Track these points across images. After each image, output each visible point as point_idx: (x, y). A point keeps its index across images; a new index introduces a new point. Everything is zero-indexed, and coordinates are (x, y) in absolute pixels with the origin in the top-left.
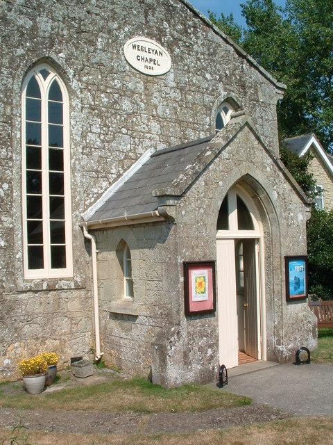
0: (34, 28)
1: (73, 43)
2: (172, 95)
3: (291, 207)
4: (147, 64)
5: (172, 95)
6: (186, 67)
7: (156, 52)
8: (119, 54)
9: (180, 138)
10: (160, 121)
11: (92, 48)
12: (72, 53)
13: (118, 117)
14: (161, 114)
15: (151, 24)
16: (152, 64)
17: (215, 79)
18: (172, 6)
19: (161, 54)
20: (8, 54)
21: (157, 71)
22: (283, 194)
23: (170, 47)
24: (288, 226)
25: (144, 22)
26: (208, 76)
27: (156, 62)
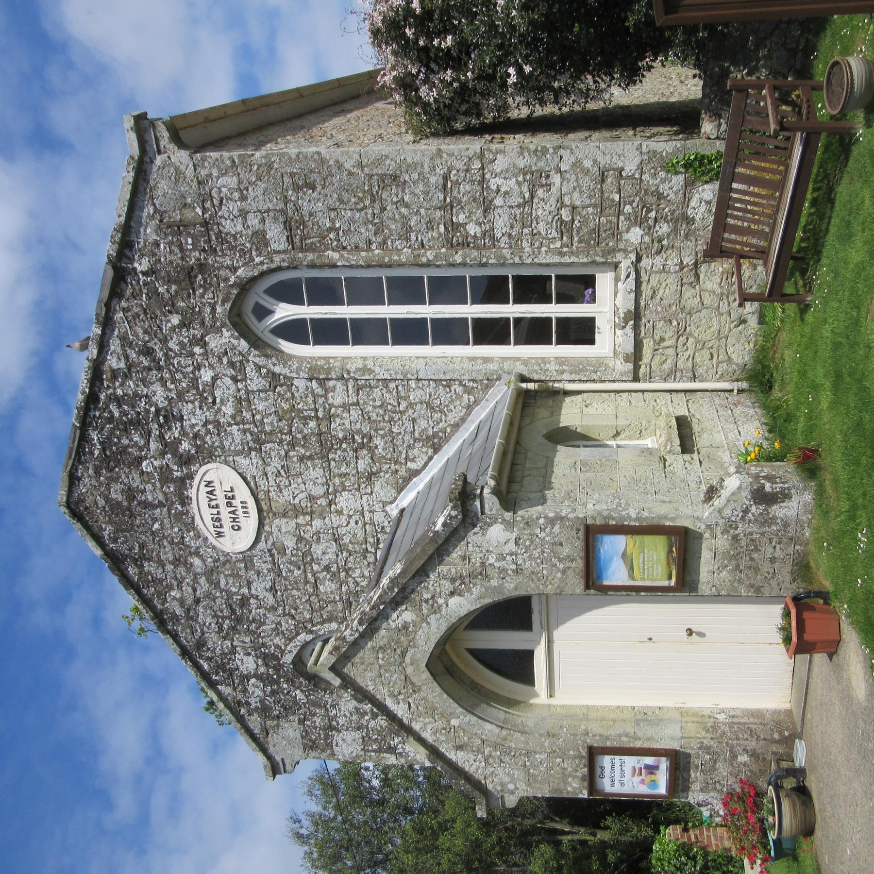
0: (257, 676)
1: (258, 628)
2: (276, 464)
3: (476, 559)
4: (240, 512)
5: (276, 464)
6: (210, 427)
7: (211, 493)
8: (247, 558)
9: (356, 451)
10: (336, 491)
11: (252, 601)
12: (273, 630)
13: (350, 565)
14: (319, 491)
15: (161, 497)
16: (236, 503)
17: (205, 355)
18: (104, 450)
19: (209, 484)
20: (309, 709)
21: (243, 493)
22: (453, 580)
23: (186, 460)
25: (165, 509)
26: (206, 375)
27: (230, 494)
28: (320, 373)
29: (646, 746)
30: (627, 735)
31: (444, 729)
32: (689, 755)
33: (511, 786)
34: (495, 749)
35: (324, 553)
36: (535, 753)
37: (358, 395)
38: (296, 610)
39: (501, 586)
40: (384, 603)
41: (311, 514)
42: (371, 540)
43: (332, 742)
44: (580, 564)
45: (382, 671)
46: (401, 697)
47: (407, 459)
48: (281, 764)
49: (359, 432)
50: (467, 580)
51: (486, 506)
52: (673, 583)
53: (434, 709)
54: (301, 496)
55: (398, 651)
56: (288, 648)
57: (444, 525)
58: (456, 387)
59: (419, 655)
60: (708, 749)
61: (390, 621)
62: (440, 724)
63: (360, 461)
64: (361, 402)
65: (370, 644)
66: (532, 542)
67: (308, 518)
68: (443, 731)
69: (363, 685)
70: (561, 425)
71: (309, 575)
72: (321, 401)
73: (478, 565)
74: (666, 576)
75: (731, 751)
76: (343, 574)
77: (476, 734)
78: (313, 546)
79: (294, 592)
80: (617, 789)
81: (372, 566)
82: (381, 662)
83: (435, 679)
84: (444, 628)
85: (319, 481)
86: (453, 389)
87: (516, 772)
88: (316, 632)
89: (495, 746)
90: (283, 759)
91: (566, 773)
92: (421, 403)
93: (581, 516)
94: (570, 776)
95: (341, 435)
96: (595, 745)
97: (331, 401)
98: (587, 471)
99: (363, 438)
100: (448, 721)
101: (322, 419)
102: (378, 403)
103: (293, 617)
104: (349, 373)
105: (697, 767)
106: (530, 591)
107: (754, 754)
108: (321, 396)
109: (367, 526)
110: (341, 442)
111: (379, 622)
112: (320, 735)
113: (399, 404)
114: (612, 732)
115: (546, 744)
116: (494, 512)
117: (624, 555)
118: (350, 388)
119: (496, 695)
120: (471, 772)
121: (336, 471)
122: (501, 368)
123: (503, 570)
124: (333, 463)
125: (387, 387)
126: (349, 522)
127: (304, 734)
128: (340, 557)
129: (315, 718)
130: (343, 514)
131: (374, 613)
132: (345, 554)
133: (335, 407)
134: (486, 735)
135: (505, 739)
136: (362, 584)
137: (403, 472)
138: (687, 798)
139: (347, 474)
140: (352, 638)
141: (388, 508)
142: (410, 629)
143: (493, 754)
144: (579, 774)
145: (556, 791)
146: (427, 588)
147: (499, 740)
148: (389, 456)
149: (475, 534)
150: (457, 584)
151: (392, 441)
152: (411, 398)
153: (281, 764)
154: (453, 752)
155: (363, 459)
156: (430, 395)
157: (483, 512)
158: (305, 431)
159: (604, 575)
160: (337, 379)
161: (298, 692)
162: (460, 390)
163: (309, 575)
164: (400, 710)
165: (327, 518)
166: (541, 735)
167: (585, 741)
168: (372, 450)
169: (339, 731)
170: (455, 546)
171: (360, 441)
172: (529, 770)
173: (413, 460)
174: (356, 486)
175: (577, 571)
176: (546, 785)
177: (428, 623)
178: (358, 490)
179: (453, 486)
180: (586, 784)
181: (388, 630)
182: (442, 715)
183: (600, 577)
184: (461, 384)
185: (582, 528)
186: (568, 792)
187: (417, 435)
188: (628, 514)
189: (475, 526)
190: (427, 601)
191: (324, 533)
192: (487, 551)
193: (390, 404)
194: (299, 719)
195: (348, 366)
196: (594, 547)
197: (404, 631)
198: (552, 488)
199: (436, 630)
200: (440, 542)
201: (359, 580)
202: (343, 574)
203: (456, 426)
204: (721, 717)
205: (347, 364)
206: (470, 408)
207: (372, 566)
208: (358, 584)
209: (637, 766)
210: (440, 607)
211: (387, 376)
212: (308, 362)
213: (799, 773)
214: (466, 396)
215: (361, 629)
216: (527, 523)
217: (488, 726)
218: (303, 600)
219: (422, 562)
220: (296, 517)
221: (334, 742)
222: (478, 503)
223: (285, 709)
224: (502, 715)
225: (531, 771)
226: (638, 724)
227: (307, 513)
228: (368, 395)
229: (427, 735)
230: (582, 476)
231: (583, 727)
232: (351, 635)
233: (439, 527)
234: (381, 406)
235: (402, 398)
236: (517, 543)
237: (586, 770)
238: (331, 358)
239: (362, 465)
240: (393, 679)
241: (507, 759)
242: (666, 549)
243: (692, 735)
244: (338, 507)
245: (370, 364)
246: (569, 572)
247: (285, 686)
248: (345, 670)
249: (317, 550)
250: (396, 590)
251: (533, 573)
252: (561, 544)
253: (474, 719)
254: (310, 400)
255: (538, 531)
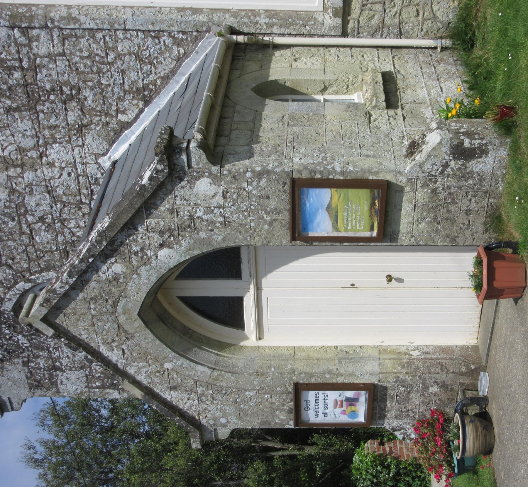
3: (184, 212)
9: (65, 102)
10: (46, 144)
13: (65, 216)
14: (29, 143)
20: (32, 352)
22: (162, 233)
24: (226, 223)
28: (21, 21)
29: (346, 381)
30: (330, 372)
31: (158, 372)
32: (386, 388)
33: (223, 421)
34: (207, 388)
35: (37, 205)
36: (245, 390)
37: (64, 45)
38: (13, 259)
39: (209, 238)
40: (93, 256)
41: (22, 166)
42: (85, 191)
43: (56, 382)
44: (286, 216)
45: (95, 321)
46: (115, 344)
47: (117, 111)
48: (8, 403)
49: (67, 83)
50: (176, 233)
51: (193, 160)
52: (374, 234)
53: (147, 354)
54: (11, 148)
55: (110, 302)
56: (8, 296)
57: (151, 178)
58: (165, 39)
59: (130, 304)
60: (402, 383)
61: (100, 273)
62: (154, 367)
63: (70, 113)
64: (68, 52)
65: (81, 296)
66: (239, 195)
67: (19, 170)
68: (157, 374)
69: (76, 334)
70: (271, 79)
71: (24, 227)
72: (25, 50)
73: (186, 217)
74: (368, 228)
75: (423, 384)
76: (58, 225)
77: (189, 376)
78: (27, 198)
79: (10, 243)
80: (321, 419)
81: (87, 217)
82: (93, 312)
83: (147, 326)
84: (154, 279)
85: (29, 133)
86: (162, 40)
87: (228, 408)
88: (34, 281)
89: (208, 385)
90: (9, 399)
91: (274, 407)
92: (130, 55)
93: (288, 169)
94: (278, 409)
95: (48, 87)
96: (301, 382)
97: (35, 50)
98: (294, 125)
99: (71, 90)
100: (162, 365)
101: (27, 70)
102: (86, 54)
103: (10, 267)
104: (53, 21)
105: (392, 398)
106: (238, 243)
107: (443, 386)
108: (25, 46)
109: (80, 178)
110: (49, 93)
111: (89, 274)
112: (44, 375)
113: (107, 54)
114: (316, 370)
115: (255, 382)
116: (201, 165)
117: (329, 208)
118: (55, 37)
119: (208, 339)
120: (185, 409)
121: (46, 123)
122: (211, 20)
123: (211, 223)
124: (41, 115)
125: (93, 37)
126: (61, 174)
127: (29, 375)
128: (54, 208)
129: (39, 360)
130: (54, 166)
131: (84, 266)
132: (59, 205)
133: (41, 57)
134: (198, 376)
135: (216, 379)
136: (78, 234)
137: (114, 125)
138: (383, 425)
139: (57, 126)
140: (63, 290)
141: (100, 161)
142: (121, 280)
143: (206, 392)
144: (286, 407)
145: (265, 423)
146: (135, 241)
147: (211, 381)
148: (99, 108)
149: (182, 187)
150: (166, 236)
151: (101, 93)
152: (119, 49)
153: (8, 403)
154: (167, 393)
155: (72, 110)
156: (139, 47)
157: (190, 166)
158: (10, 82)
159: (310, 227)
160: (41, 28)
161: (20, 337)
162: (169, 41)
163: (24, 227)
164: (114, 356)
165: (39, 170)
166: (250, 375)
167: (291, 378)
168: (81, 102)
169: (63, 371)
170: (163, 200)
171: (68, 92)
172: (239, 405)
173: (123, 113)
174: (67, 138)
175: (284, 223)
176: (256, 418)
177: (138, 275)
178: (69, 141)
179: (159, 140)
180: (292, 416)
181: (98, 281)
182: (156, 360)
183: (305, 229)
184: (170, 36)
185: (288, 181)
186: (276, 424)
187: (127, 87)
188: (333, 168)
189: (182, 180)
190: (136, 254)
191: (36, 185)
192: (195, 204)
193: (97, 55)
194: (23, 362)
195: (52, 15)
196: (300, 200)
197: (115, 282)
198: (259, 142)
199: (146, 281)
200: (147, 195)
201: (74, 230)
202: (58, 225)
203: (166, 79)
204: (416, 354)
205: (50, 12)
206: (180, 60)
207: (87, 217)
208: (73, 234)
209: (339, 399)
210: (149, 259)
211: (93, 26)
212: (9, 10)
213: (482, 401)
214: (175, 48)
215: (71, 281)
216: (234, 177)
217: (200, 368)
218: (20, 251)
219: (130, 215)
220: (7, 169)
221: (59, 381)
222: (184, 157)
223: (9, 353)
224: (213, 358)
225: (242, 406)
226: (340, 362)
227: (18, 166)
228: (75, 46)
229: (142, 378)
230: (289, 130)
231: (290, 366)
232: (61, 287)
233: (145, 181)
234: (88, 57)
235: (109, 49)
236: (224, 197)
237: (292, 403)
238: (33, 5)
239: (72, 117)
240: (106, 327)
241: (219, 397)
242: (369, 202)
243: (389, 370)
244: (50, 159)
245: (75, 13)
246: (276, 224)
247: (7, 332)
248: (58, 321)
249: (31, 202)
250: (104, 243)
251: (240, 225)
252: (268, 197)
253: (186, 362)
254: (13, 49)
255: (245, 185)
